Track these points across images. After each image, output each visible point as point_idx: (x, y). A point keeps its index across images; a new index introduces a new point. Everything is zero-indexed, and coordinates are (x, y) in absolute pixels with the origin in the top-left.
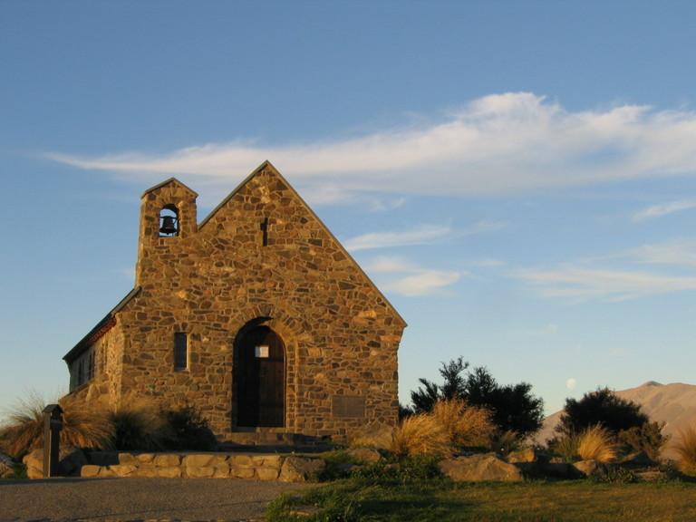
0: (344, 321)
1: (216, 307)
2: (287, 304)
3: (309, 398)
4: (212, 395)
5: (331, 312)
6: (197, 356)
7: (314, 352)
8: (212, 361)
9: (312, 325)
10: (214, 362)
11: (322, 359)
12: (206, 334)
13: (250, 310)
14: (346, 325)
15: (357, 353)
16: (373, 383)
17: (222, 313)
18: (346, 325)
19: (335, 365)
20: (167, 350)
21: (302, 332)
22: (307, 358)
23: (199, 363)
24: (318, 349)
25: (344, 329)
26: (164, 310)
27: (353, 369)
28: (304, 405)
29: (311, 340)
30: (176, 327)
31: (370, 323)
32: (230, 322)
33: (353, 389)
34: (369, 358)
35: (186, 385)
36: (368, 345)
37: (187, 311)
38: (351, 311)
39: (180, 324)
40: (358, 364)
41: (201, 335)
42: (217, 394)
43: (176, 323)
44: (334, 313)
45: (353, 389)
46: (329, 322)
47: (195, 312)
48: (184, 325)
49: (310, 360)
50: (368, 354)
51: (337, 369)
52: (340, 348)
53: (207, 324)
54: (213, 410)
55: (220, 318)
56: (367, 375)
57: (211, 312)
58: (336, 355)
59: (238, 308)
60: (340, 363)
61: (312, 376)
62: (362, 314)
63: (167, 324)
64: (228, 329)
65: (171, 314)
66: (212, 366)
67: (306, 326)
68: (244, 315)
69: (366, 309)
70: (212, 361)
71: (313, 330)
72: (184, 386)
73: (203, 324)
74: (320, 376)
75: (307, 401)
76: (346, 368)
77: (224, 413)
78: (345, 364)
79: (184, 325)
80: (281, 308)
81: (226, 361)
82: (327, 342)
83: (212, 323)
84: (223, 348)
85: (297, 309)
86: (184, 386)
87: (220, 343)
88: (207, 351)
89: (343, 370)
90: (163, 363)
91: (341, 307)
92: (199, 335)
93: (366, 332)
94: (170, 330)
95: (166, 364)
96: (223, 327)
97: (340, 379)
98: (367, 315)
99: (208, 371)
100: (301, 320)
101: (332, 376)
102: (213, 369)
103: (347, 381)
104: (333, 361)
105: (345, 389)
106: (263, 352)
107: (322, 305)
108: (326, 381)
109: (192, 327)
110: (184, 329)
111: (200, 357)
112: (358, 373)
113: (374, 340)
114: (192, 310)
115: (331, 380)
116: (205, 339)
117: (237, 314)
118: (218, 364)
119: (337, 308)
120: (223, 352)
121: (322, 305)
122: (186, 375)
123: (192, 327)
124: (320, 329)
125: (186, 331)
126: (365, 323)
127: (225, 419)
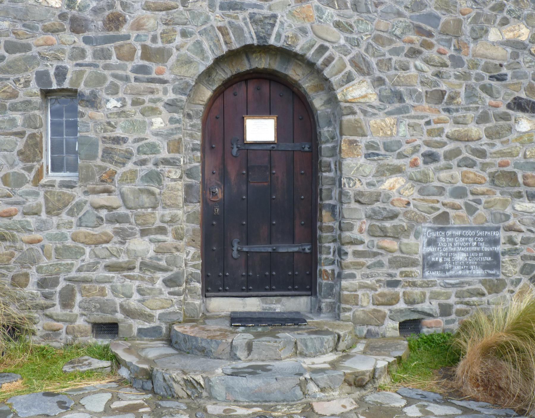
0: (451, 51)
1: (138, 26)
2: (315, 14)
3: (366, 239)
4: (133, 235)
5: (420, 31)
6: (93, 144)
7: (381, 126)
8: (128, 155)
9: (373, 61)
10: (134, 159)
11: (399, 144)
12: (114, 90)
13: (220, 28)
14: (457, 62)
15: (483, 127)
16: (519, 195)
17: (154, 39)
18: (457, 62)
19: (430, 158)
20: (21, 134)
21: (349, 79)
22: (363, 141)
23: (98, 162)
24: (390, 120)
25: (451, 71)
26: (12, 38)
27: (472, 165)
28: (356, 253)
29: (373, 99)
30: (42, 77)
31: (515, 55)
32: (172, 60)
33: (471, 210)
34: (513, 136)
35: (71, 213)
36: (509, 106)
37: (68, 37)
38: (467, 28)
39: (52, 72)
40: (482, 154)
41: (103, 95)
42: (144, 233)
43: (41, 68)
44: (430, 34)
45: (471, 210)
46: (414, 53)
47: (87, 40)
48: (61, 73)
49: (369, 146)
50: (510, 129)
51: (432, 166)
52: (444, 115)
53: (119, 67)
54: (136, 272)
55: (147, 54)
56: (505, 178)
57: (128, 37)
58: (430, 133)
59: (190, 28)
60: (441, 152)
61: (369, 184)
62: (494, 35)
63: (19, 71)
64: (167, 76)
65: (27, 48)
66: (130, 166)
67: (361, 67)
68: (206, 45)
69: (505, 22)
70: (128, 155)
71: (377, 74)
72: (65, 217)
73: (107, 67)
74: (393, 184)
75: (362, 242)
76: (454, 162)
77: (161, 276)
78: (456, 152)
79: (61, 73)
80: (297, 24)
81: (164, 154)
82: (408, 102)
83: (130, 65)
84: (158, 123)
85: (338, 25)
86: (65, 217)
87: (154, 111)
88: (119, 133)
89: (449, 168)
90: (12, 165)
91: (444, 19)
92: (94, 95)
93: (501, 78)
94: (27, 83)
95: (19, 168)
96: (154, 75)
97: (441, 191)
98: (509, 36)
99: (122, 180)
100: (346, 52)
101: (421, 182)
102: (134, 173)
103: (459, 193)
104: (425, 149)
105: (452, 213)
106: (260, 130)
107: (399, 14)
108: (411, 193)
109: (79, 75)
110: (59, 82)
111: (101, 147)
112: (485, 175)
113: (523, 95)
114: (82, 35)
115: (421, 191)
116: (113, 103)
117: (190, 41)
118: (143, 162)
119: (432, 18)
120: (156, 134)
121: (399, 14)
122: (68, 191)
123: (82, 73)
124: (392, 72)
125: (66, 85)
126: (502, 54)
127: (166, 290)
